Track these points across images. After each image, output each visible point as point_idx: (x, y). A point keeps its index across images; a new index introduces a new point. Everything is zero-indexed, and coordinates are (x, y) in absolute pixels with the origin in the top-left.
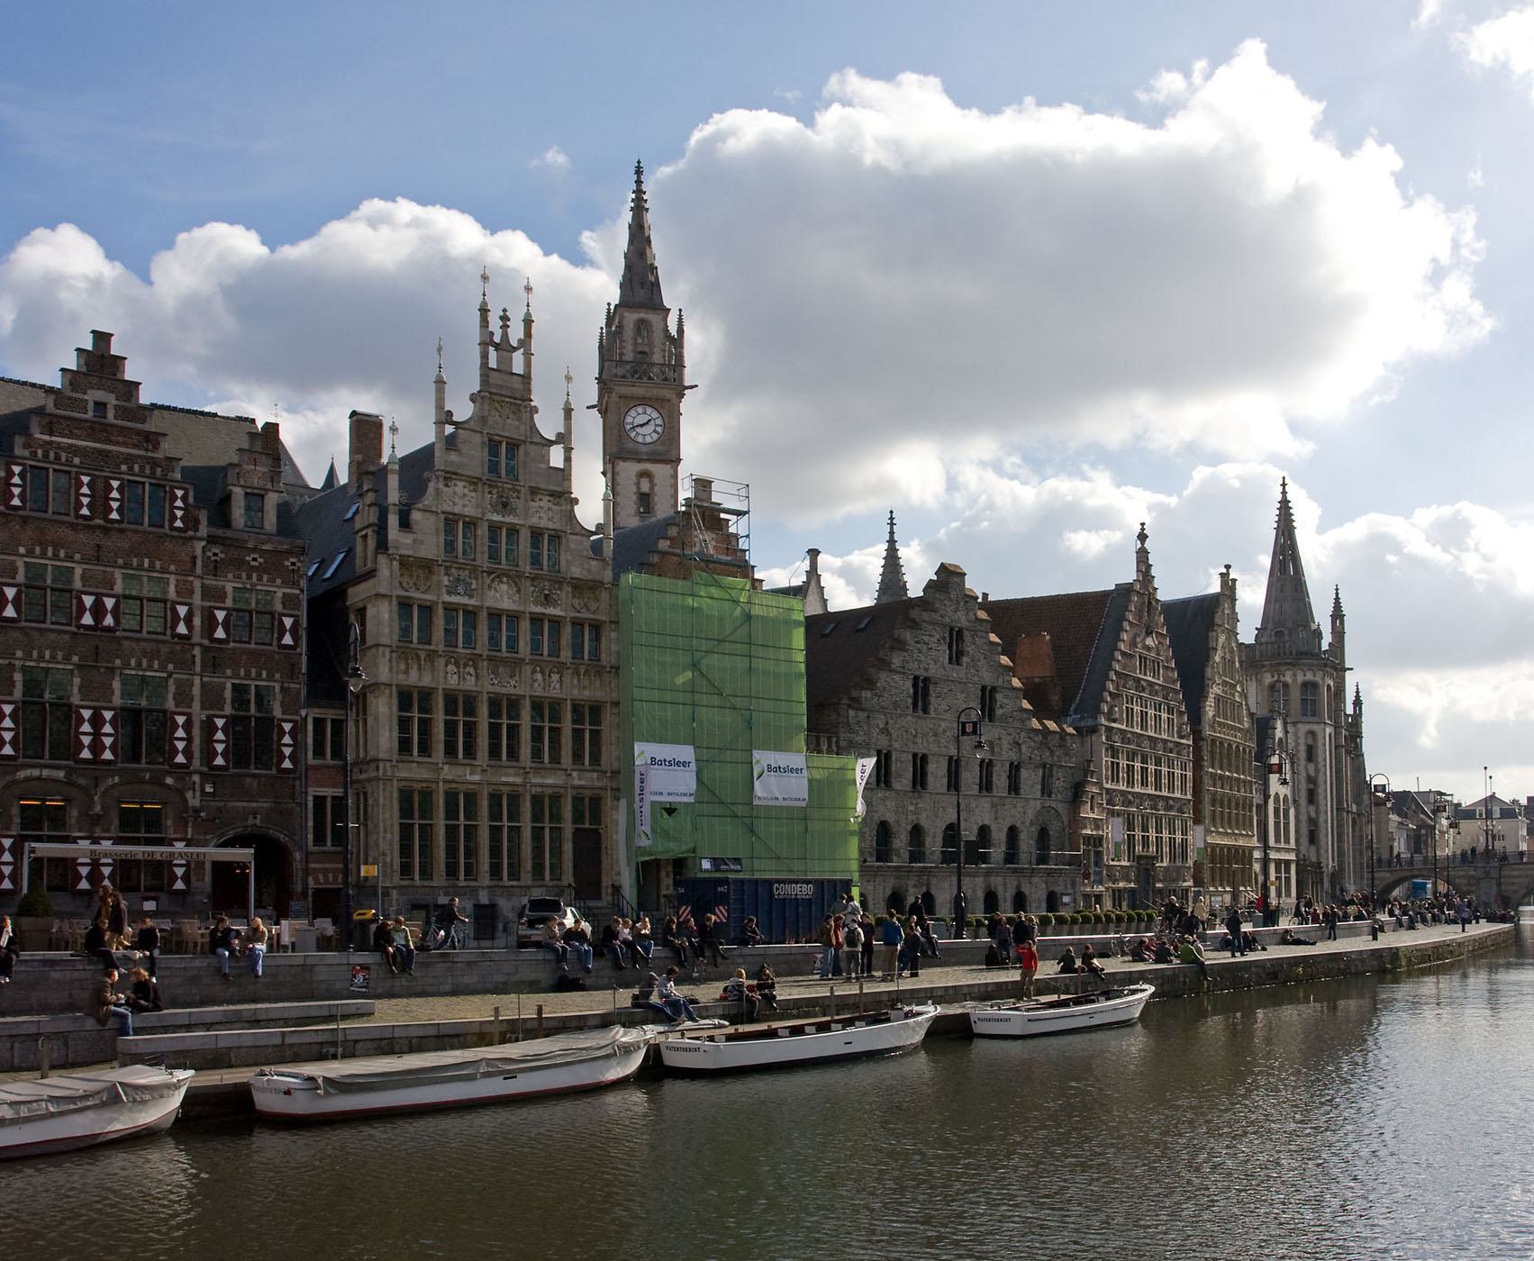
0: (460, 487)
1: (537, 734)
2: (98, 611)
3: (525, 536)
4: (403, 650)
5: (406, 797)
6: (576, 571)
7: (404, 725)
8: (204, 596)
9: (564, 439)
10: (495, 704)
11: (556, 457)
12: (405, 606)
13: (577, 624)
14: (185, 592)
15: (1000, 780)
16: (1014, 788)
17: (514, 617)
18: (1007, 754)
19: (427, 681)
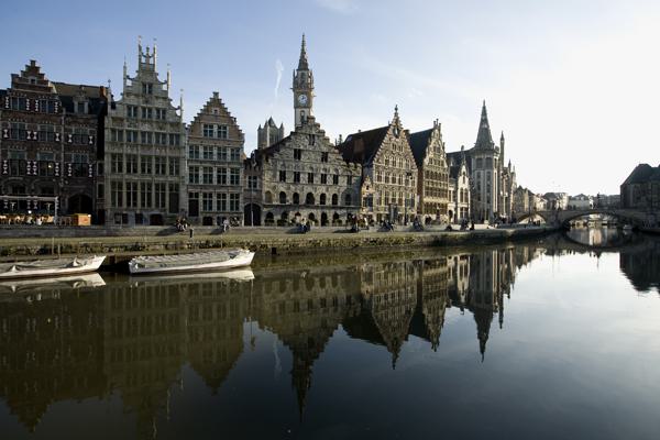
0: (132, 97)
1: (157, 166)
2: (32, 135)
3: (154, 113)
4: (113, 143)
5: (113, 183)
6: (171, 120)
7: (113, 164)
8: (65, 130)
9: (166, 82)
10: (143, 158)
11: (164, 87)
12: (113, 131)
13: (171, 135)
14: (59, 130)
15: (330, 180)
16: (336, 180)
17: (150, 134)
18: (332, 172)
19: (121, 151)
